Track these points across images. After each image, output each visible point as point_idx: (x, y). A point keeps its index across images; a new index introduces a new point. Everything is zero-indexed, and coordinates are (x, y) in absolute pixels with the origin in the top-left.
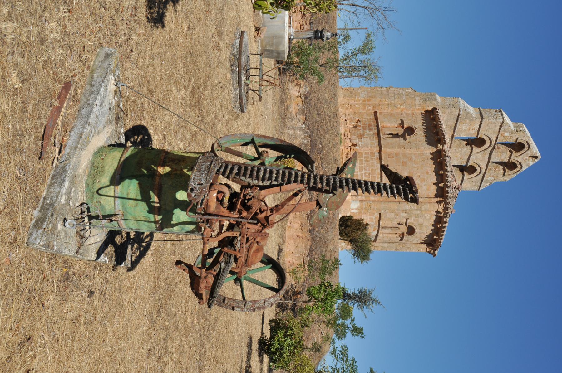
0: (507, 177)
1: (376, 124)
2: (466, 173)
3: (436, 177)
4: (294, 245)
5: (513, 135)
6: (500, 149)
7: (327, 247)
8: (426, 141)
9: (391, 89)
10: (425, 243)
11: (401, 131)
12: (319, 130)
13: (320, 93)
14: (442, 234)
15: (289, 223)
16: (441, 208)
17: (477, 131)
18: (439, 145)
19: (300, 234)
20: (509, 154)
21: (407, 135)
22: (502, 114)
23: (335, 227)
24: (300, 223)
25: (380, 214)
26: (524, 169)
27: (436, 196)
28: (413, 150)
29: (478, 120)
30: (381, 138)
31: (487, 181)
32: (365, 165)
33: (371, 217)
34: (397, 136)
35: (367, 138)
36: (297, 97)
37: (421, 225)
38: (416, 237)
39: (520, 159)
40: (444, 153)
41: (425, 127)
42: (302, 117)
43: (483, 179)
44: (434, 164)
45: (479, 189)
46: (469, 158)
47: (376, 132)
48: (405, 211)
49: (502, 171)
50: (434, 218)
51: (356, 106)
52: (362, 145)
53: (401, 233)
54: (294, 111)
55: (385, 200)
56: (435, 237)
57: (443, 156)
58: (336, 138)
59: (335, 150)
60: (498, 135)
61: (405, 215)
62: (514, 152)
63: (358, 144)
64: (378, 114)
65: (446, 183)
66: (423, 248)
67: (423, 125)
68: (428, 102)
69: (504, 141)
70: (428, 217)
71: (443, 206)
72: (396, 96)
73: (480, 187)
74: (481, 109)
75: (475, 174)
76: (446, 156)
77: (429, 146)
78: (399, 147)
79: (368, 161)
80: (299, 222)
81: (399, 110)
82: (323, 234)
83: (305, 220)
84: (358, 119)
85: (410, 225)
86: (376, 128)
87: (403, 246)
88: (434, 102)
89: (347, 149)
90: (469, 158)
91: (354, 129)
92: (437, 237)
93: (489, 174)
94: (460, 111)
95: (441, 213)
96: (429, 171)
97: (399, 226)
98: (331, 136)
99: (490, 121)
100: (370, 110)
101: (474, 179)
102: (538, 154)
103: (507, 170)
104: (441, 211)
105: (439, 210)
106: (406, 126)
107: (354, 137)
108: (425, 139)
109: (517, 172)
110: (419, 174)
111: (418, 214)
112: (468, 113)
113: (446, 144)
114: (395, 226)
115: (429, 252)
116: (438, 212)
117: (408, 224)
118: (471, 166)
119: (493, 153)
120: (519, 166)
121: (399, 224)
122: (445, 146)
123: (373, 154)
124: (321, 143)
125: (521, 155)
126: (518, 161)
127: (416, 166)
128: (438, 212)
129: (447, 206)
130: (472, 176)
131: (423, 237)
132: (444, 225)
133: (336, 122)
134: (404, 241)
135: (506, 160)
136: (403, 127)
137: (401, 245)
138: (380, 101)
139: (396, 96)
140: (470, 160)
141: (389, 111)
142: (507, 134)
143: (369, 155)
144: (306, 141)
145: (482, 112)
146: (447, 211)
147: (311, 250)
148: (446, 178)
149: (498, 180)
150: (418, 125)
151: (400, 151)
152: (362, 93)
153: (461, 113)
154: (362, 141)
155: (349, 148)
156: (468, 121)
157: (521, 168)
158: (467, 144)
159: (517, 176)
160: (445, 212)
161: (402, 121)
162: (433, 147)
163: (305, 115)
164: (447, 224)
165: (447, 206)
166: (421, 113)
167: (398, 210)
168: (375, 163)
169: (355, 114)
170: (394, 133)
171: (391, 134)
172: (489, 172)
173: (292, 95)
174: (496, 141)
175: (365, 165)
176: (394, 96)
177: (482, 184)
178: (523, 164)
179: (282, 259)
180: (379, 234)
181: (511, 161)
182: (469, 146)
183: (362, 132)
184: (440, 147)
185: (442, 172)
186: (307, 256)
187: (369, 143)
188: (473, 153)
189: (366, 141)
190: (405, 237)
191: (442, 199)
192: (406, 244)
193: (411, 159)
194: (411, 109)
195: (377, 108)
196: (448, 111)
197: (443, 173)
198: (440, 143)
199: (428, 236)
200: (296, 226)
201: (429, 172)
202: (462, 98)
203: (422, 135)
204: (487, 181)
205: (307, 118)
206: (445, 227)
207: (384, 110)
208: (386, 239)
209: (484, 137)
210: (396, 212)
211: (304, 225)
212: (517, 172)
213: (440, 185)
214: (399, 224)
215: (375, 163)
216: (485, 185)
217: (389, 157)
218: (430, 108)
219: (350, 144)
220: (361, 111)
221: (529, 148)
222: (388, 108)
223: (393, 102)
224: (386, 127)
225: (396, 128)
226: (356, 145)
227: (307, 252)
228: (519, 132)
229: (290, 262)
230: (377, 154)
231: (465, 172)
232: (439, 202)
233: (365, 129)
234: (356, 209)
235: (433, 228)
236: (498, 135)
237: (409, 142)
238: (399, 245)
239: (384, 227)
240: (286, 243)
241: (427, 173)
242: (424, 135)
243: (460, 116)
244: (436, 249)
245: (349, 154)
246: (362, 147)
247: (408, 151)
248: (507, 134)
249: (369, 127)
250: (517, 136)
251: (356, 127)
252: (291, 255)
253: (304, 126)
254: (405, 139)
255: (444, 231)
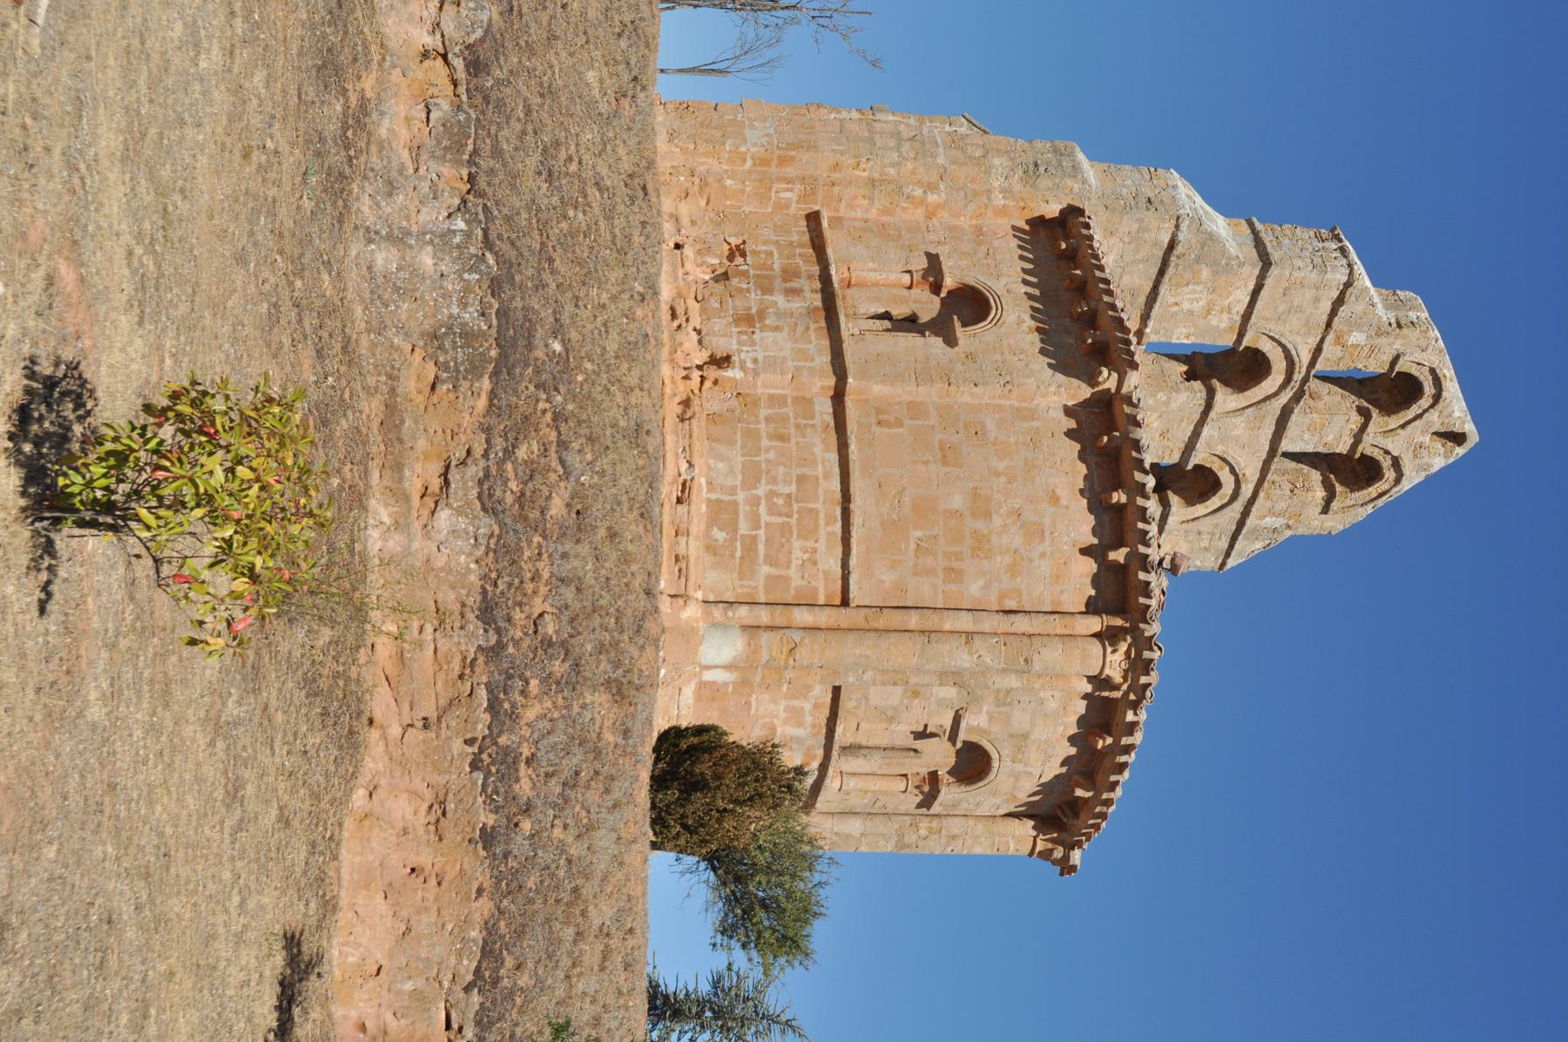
0: (1338, 517)
1: (816, 269)
2: (1174, 500)
3: (1091, 520)
4: (389, 921)
5: (1383, 341)
6: (1320, 398)
7: (584, 913)
8: (1043, 352)
9: (879, 116)
10: (1030, 817)
11: (928, 306)
12: (551, 260)
13: (559, 58)
14: (1113, 778)
15: (359, 795)
16: (1115, 664)
17: (1238, 319)
18: (1105, 372)
19: (425, 859)
20: (1356, 420)
21: (957, 324)
22: (1343, 250)
23: (630, 796)
24: (429, 796)
25: (837, 691)
26: (1406, 485)
27: (1092, 608)
28: (989, 394)
29: (1247, 270)
30: (845, 334)
31: (1256, 534)
32: (771, 455)
33: (795, 703)
34: (910, 323)
35: (777, 329)
36: (425, 55)
37: (1021, 739)
38: (995, 793)
39: (1396, 445)
40: (1127, 409)
41: (1037, 292)
42: (452, 175)
43: (1241, 524)
44: (1082, 457)
45: (1223, 564)
46: (1196, 434)
47: (818, 303)
48: (954, 677)
49: (1320, 493)
50: (1081, 707)
51: (729, 182)
52: (755, 361)
53: (924, 771)
54: (404, 135)
55: (862, 623)
56: (1079, 792)
57: (1121, 422)
58: (639, 313)
59: (636, 373)
60: (1322, 341)
61: (949, 692)
62: (1375, 413)
63: (735, 358)
64: (825, 224)
65: (1142, 549)
66: (1019, 840)
67: (1025, 282)
68: (1044, 183)
69: (1342, 367)
70: (1053, 705)
71: (1128, 653)
72: (906, 147)
73: (1228, 554)
74: (1259, 226)
75: (1215, 502)
76: (1138, 425)
77: (1060, 377)
78: (923, 375)
79: (783, 438)
80: (422, 787)
81: (919, 213)
82: (562, 848)
83: (459, 777)
84: (734, 241)
85: (973, 738)
86: (818, 285)
87: (930, 830)
88: (1069, 182)
89: (686, 378)
90: (1196, 434)
91: (719, 288)
92: (1090, 794)
93: (1269, 504)
94: (1177, 226)
95: (1117, 688)
96: (1058, 491)
97: (919, 744)
98: (614, 298)
99: (1298, 275)
100: (787, 206)
101: (1206, 525)
102: (1469, 428)
103: (1339, 488)
104: (1117, 678)
105: (1107, 671)
106: (949, 282)
107: (718, 324)
108: (1039, 345)
109: (1380, 495)
110: (1017, 503)
111: (1009, 692)
112: (1211, 238)
113: (1134, 366)
114: (899, 742)
115: (1046, 855)
116: (1100, 681)
117: (962, 736)
118: (1198, 468)
119: (1294, 417)
120: (1390, 475)
121: (921, 735)
122: (1133, 379)
123: (804, 403)
124: (557, 331)
125: (1403, 426)
126: (1387, 452)
127: (1001, 466)
128: (1100, 681)
129: (1147, 654)
130: (1200, 509)
131: (1025, 790)
132: (1125, 741)
133: (644, 224)
134: (936, 808)
135: (1343, 448)
136: (936, 288)
137: (924, 825)
138: (836, 167)
139: (906, 147)
140: (1201, 445)
141: (873, 213)
142: (1357, 338)
143: (789, 411)
144: (470, 315)
145: (1263, 235)
146: (1143, 680)
147: (489, 952)
148: (1140, 525)
149: (1302, 531)
150: (1003, 281)
151: (929, 394)
152: (752, 127)
153: (1181, 237)
154: (753, 343)
155: (696, 374)
156: (1205, 273)
157: (1398, 481)
158: (1190, 376)
159: (1377, 512)
160: (1135, 680)
161: (933, 260)
162: (1075, 382)
163: (471, 162)
164: (1137, 738)
165: (1147, 654)
166: (1014, 228)
167: (918, 671)
168: (818, 449)
169: (721, 219)
170: (899, 311)
171: (886, 316)
172: (1268, 497)
173: (393, 44)
174: (1312, 363)
175: (771, 455)
176: (898, 148)
177: (1237, 546)
178: (1407, 466)
179: (315, 1014)
180: (827, 781)
181: (1360, 449)
182: (1197, 385)
183: (754, 299)
184: (1108, 380)
185: (1119, 497)
186: (467, 989)
187: (787, 353)
188: (1212, 414)
189: (773, 343)
190: (943, 790)
191: (1118, 622)
192: (945, 822)
193: (979, 433)
194: (971, 208)
195: (820, 194)
196: (1128, 224)
197: (1124, 499)
198: (1112, 366)
199: (1046, 789)
200: (406, 809)
201: (1063, 493)
202: (1183, 175)
203: (1025, 327)
204: (1256, 534)
205: (482, 182)
206: (1128, 749)
207: (852, 207)
208: (856, 802)
209: (1267, 347)
210: (913, 680)
211: (451, 806)
212: (1380, 495)
213: (1112, 556)
214: (921, 735)
215: (818, 449)
216: (1247, 547)
217: (879, 423)
218: (1052, 210)
219: (700, 357)
220: (747, 209)
221: (1437, 398)
222: (871, 199)
223: (892, 171)
224: (862, 285)
225: (905, 292)
226: (727, 359)
227: (469, 965)
228: (1405, 331)
229: (363, 1028)
230: (825, 408)
231: (1170, 494)
232: (1108, 637)
233: (767, 290)
234: (727, 667)
235: (1073, 751)
236: (1322, 341)
237: (969, 356)
238: (915, 826)
239: (849, 749)
240: (344, 916)
241: (1055, 499)
242: (1033, 324)
243: (1179, 250)
244: (1079, 844)
245: (696, 402)
246: (756, 373)
247: (965, 396)
248: (1357, 338)
249: (785, 280)
250: (1398, 346)
251: (725, 276)
252: (372, 983)
253: (460, 224)
254: (951, 341)
255: (1124, 766)
